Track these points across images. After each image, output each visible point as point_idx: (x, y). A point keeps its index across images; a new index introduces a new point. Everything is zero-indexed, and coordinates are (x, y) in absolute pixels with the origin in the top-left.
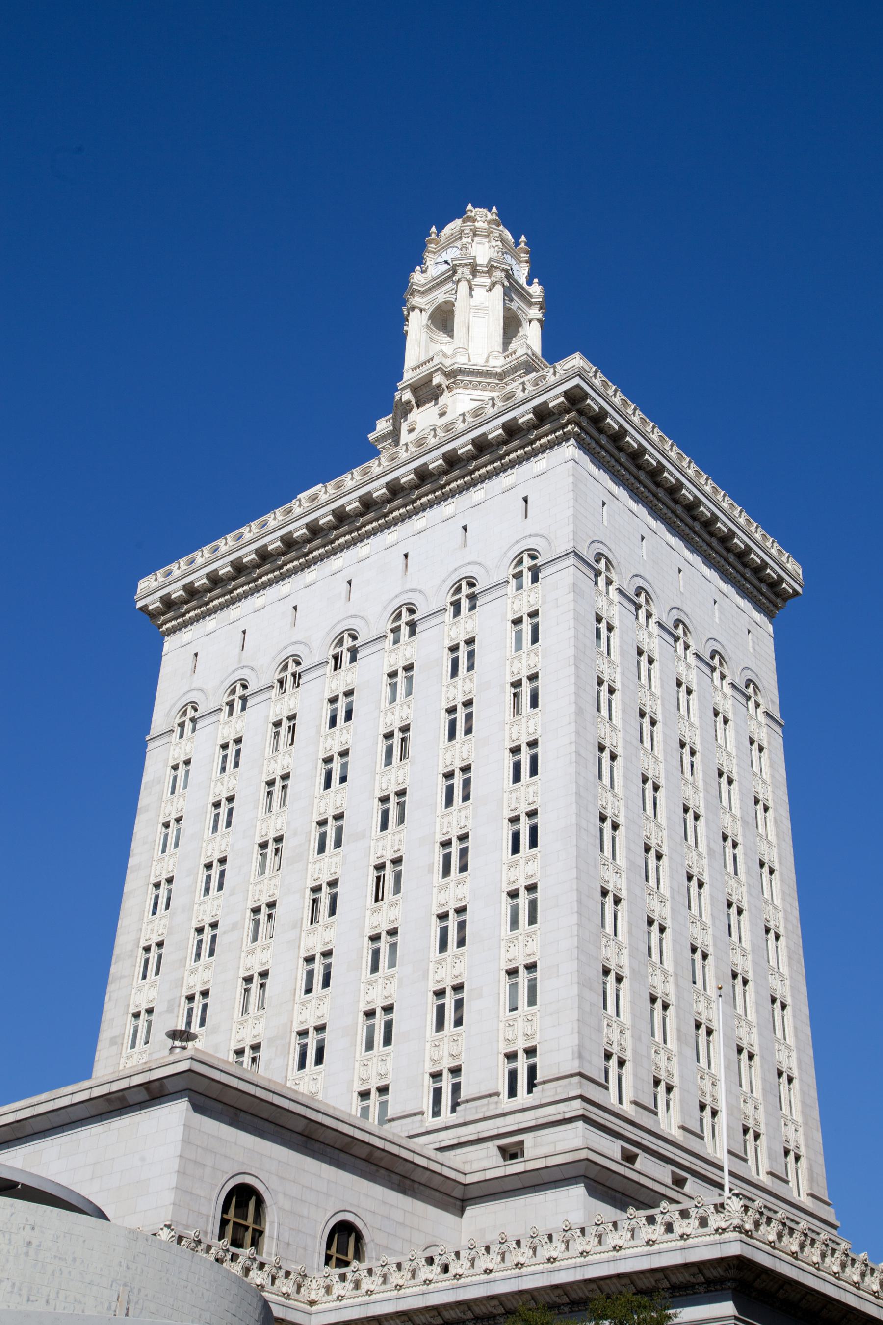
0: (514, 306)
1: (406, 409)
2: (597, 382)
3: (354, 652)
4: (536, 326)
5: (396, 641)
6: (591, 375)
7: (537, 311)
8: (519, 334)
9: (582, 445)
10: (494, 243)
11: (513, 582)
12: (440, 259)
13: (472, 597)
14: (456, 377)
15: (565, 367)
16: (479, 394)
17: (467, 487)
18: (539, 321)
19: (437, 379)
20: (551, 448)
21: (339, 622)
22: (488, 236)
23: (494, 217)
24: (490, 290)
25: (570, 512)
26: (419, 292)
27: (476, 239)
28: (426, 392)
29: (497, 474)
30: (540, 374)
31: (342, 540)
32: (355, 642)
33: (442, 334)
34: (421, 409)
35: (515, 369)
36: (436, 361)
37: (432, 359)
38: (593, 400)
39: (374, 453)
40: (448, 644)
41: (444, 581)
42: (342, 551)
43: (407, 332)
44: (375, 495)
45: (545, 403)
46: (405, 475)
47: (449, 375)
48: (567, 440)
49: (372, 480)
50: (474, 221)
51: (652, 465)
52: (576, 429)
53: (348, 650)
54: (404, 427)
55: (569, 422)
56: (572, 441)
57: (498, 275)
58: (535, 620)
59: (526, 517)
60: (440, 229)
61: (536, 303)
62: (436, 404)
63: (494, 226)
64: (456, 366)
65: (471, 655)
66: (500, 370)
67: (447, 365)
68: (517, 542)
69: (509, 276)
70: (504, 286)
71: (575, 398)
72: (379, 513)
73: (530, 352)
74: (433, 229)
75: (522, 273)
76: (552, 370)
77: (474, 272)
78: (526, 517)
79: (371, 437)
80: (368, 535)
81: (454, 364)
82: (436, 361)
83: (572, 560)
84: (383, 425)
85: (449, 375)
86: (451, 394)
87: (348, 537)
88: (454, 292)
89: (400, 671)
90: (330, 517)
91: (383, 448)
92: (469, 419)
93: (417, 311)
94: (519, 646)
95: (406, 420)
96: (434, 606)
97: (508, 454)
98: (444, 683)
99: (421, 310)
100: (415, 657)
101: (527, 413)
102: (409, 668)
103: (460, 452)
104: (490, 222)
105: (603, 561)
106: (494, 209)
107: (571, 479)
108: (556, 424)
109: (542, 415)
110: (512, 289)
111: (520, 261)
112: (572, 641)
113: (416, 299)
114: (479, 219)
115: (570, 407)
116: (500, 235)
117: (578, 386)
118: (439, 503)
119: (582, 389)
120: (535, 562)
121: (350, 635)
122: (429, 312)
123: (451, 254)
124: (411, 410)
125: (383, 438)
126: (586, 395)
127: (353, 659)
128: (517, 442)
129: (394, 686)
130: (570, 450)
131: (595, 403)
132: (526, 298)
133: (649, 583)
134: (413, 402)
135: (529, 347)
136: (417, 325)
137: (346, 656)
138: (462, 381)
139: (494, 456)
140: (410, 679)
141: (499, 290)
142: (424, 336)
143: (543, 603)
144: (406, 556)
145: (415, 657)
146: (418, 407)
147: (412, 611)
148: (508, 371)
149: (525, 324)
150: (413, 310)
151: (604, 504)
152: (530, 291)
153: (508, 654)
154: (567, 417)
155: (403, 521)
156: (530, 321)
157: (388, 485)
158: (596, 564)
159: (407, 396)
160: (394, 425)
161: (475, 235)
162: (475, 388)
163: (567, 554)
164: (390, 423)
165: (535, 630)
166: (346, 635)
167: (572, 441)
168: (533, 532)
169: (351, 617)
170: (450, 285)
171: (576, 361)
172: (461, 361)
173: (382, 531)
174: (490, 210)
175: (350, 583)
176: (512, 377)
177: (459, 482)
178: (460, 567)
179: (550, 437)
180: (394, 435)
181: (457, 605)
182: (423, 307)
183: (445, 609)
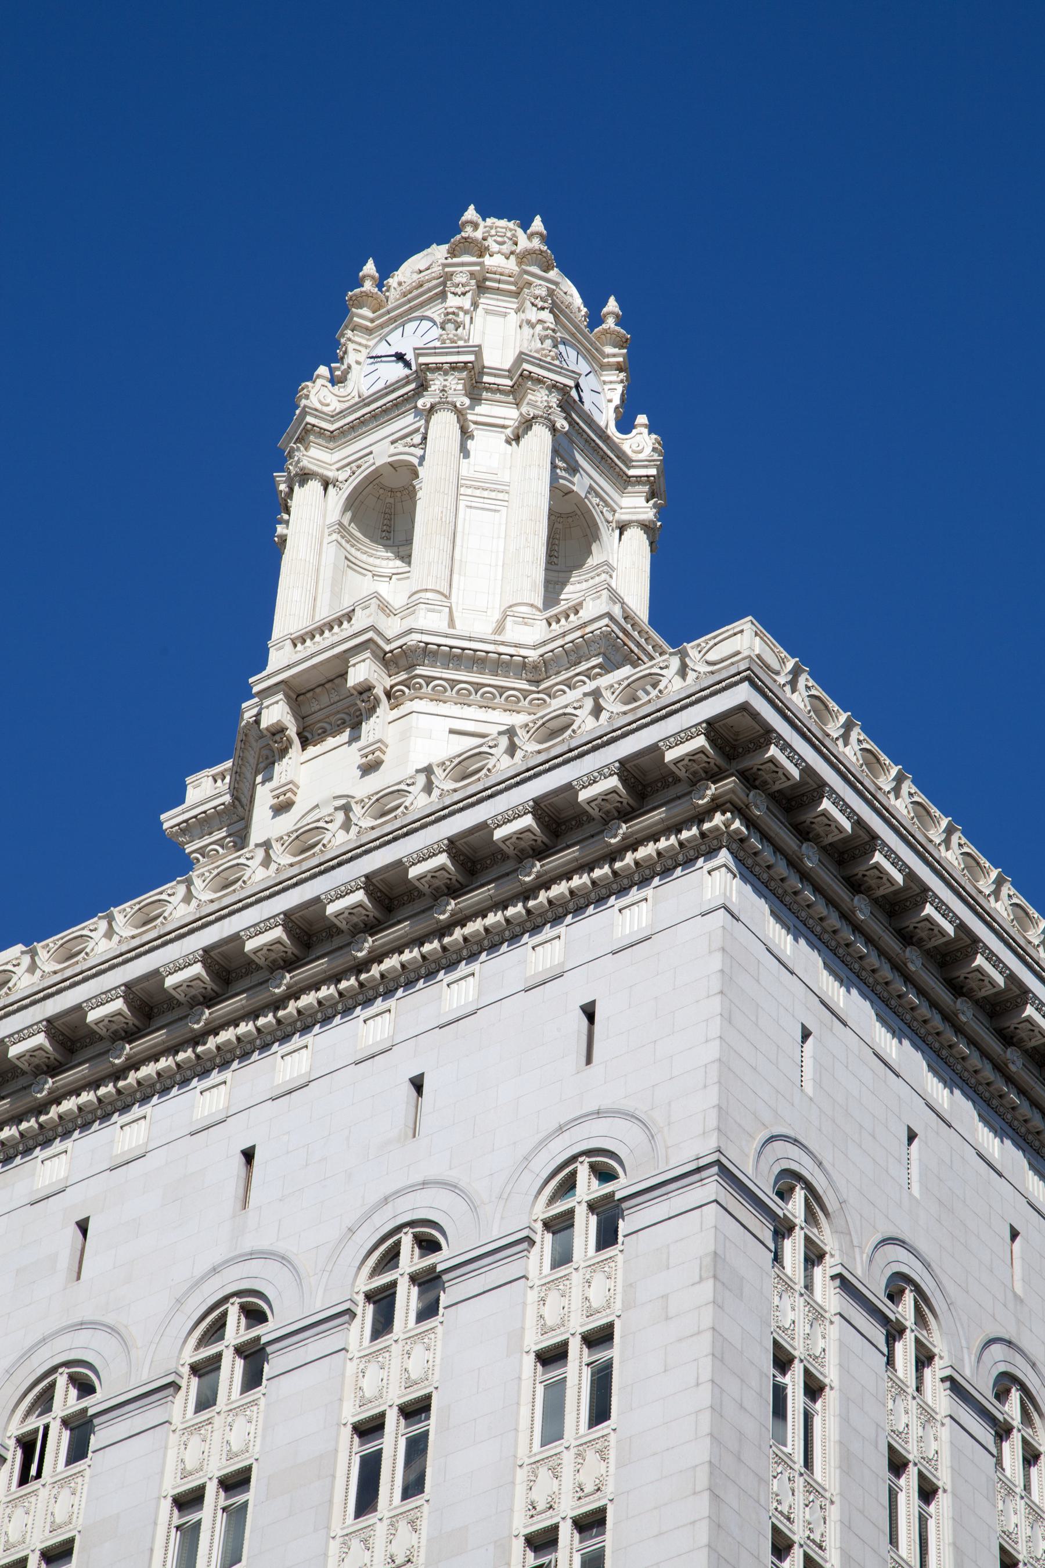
0: (579, 485)
1: (271, 748)
2: (798, 701)
3: (81, 1429)
4: (637, 544)
5: (206, 1402)
6: (782, 679)
7: (641, 501)
8: (591, 562)
9: (749, 869)
10: (533, 315)
11: (546, 1242)
12: (383, 349)
13: (429, 1282)
14: (412, 667)
15: (712, 656)
17: (428, 970)
18: (647, 527)
19: (362, 671)
20: (666, 872)
21: (44, 1340)
22: (517, 294)
23: (536, 243)
24: (517, 439)
25: (713, 1050)
26: (321, 433)
28: (330, 706)
29: (514, 938)
30: (642, 670)
31: (69, 1105)
32: (87, 1402)
33: (382, 552)
34: (312, 751)
35: (573, 655)
36: (360, 621)
37: (349, 616)
38: (785, 746)
39: (175, 864)
40: (352, 1413)
41: (352, 1231)
42: (66, 1134)
43: (284, 539)
44: (170, 981)
45: (654, 751)
46: (258, 928)
48: (711, 853)
49: (165, 940)
50: (482, 251)
51: (942, 933)
52: (737, 824)
53: (65, 1422)
54: (264, 797)
55: (717, 805)
56: (724, 856)
57: (540, 398)
58: (602, 1355)
59: (589, 1061)
60: (386, 269)
61: (639, 480)
62: (355, 738)
64: (413, 639)
65: (417, 1448)
66: (533, 655)
67: (390, 634)
68: (561, 1129)
69: (570, 404)
70: (553, 429)
71: (736, 741)
72: (180, 1032)
73: (617, 611)
74: (370, 268)
76: (675, 663)
77: (476, 390)
78: (589, 1061)
79: (170, 819)
80: (145, 1093)
81: (410, 631)
82: (360, 621)
83: (711, 1187)
84: (205, 790)
87: (87, 1097)
88: (417, 439)
89: (212, 1491)
90: (40, 1039)
91: (202, 851)
92: (444, 783)
93: (314, 486)
94: (553, 1427)
95: (268, 779)
96: (321, 1301)
98: (337, 1530)
99: (326, 484)
100: (256, 1450)
101: (602, 773)
102: (236, 1482)
103: (414, 872)
104: (523, 258)
105: (799, 1195)
107: (716, 962)
108: (680, 809)
109: (645, 782)
110: (577, 440)
111: (603, 367)
112: (706, 1418)
113: (315, 452)
114: (495, 248)
115: (720, 761)
116: (551, 293)
117: (745, 708)
118: (347, 1011)
119: (755, 716)
120: (608, 1188)
121: (73, 1379)
122: (348, 489)
124: (284, 752)
125: (204, 824)
126: (767, 735)
127: (78, 1452)
128: (571, 853)
129: (190, 1535)
130: (716, 881)
131: (790, 756)
132: (614, 466)
133: (927, 1266)
134: (292, 732)
135: (615, 597)
136: (311, 522)
137: (59, 1442)
138: (429, 680)
139: (508, 888)
140: (236, 1516)
141: (540, 439)
142: (331, 553)
143: (627, 1306)
144: (249, 1155)
145: (256, 1450)
146: (305, 743)
147: (255, 1316)
148: (556, 659)
149: (609, 536)
150: (302, 483)
151: (806, 1034)
152: (626, 447)
153: (522, 1451)
154: (712, 790)
155: (245, 1055)
156: (622, 528)
157: (208, 956)
158: (781, 1204)
159: (277, 713)
160: (235, 791)
161: (482, 288)
163: (699, 1170)
164: (223, 785)
165: (602, 1382)
166: (62, 1380)
167: (724, 856)
168: (606, 1103)
169: (81, 1326)
170: (407, 421)
171: (744, 640)
173: (185, 1082)
174: (525, 226)
175: (83, 1227)
177: (407, 956)
178: (399, 1193)
179: (663, 844)
180: (235, 818)
181: (383, 1301)
182: (330, 474)
183: (350, 1313)
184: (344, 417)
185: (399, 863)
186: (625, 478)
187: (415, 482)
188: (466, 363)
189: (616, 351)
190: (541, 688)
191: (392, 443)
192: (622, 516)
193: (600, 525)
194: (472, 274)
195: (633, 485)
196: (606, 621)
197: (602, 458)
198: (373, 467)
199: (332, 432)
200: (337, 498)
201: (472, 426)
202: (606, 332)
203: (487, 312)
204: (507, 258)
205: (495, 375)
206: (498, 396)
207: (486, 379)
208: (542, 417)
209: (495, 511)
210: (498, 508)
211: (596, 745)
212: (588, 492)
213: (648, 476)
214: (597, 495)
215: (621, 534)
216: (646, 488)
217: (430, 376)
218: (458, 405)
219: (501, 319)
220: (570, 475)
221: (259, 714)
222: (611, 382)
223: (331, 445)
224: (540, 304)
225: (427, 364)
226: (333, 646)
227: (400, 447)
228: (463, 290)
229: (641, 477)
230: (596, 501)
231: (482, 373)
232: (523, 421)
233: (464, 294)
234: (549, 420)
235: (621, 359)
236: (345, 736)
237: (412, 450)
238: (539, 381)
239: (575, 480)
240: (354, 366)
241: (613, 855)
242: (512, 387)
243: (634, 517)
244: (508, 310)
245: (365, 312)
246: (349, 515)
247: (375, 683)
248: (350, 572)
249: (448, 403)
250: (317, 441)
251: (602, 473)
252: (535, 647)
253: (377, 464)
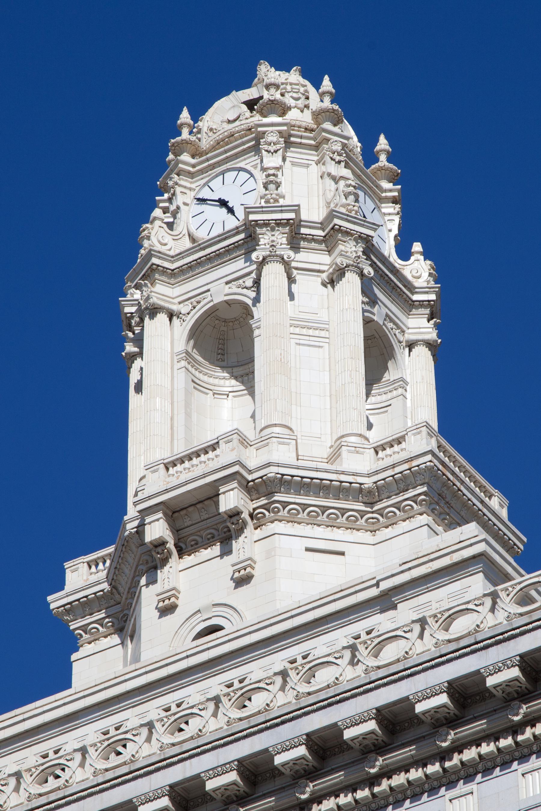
0: (378, 314)
12: (205, 194)
14: (270, 494)
18: (429, 345)
19: (231, 499)
22: (316, 148)
23: (327, 103)
26: (164, 271)
27: (293, 154)
28: (201, 522)
33: (220, 373)
34: (188, 560)
35: (402, 483)
36: (225, 455)
37: (214, 447)
46: (217, 771)
47: (255, 488)
54: (149, 597)
60: (197, 114)
61: (421, 304)
62: (226, 552)
63: (328, 126)
66: (368, 482)
69: (370, 249)
70: (362, 275)
74: (185, 116)
75: (388, 226)
77: (296, 241)
79: (56, 601)
81: (269, 465)
84: (83, 577)
85: (255, 488)
86: (259, 533)
88: (249, 282)
91: (84, 628)
93: (162, 317)
97: (459, 747)
99: (171, 315)
101: (505, 664)
104: (318, 115)
106: (327, 84)
111: (382, 200)
116: (344, 146)
123: (241, 189)
124: (165, 561)
125: (85, 606)
128: (480, 725)
132: (398, 289)
134: (171, 545)
136: (162, 351)
138: (285, 504)
141: (351, 283)
142: (181, 377)
146: (181, 553)
148: (387, 486)
149: (402, 353)
150: (152, 317)
152: (407, 273)
156: (411, 346)
159: (157, 529)
160: (113, 579)
161: (288, 144)
164: (101, 573)
170: (238, 265)
172: (279, 457)
174: (317, 85)
176: (395, 500)
182: (175, 308)
184: (183, 258)
186: (410, 302)
187: (251, 322)
188: (288, 220)
189: (390, 186)
190: (376, 508)
191: (227, 283)
192: (410, 336)
193: (395, 346)
195: (417, 308)
196: (429, 457)
197: (393, 288)
198: (211, 304)
199: (173, 270)
200: (182, 329)
201: (295, 272)
202: (381, 169)
203: (293, 164)
204: (302, 111)
205: (310, 227)
206: (313, 245)
207: (303, 231)
208: (352, 266)
209: (319, 347)
210: (321, 344)
212: (385, 320)
213: (429, 301)
214: (392, 321)
215: (410, 351)
216: (428, 311)
217: (259, 230)
218: (285, 258)
219: (304, 170)
220: (371, 307)
221: (142, 525)
222: (389, 214)
223: (172, 281)
224: (338, 158)
225: (256, 221)
226: (204, 476)
227: (234, 288)
229: (423, 301)
230: (390, 325)
231: (300, 226)
232: (337, 269)
233: (276, 152)
234: (359, 268)
235: (396, 194)
236: (216, 549)
237: (245, 291)
238: (348, 233)
239: (375, 310)
240: (182, 207)
241: (515, 730)
242: (325, 237)
244: (310, 162)
245: (185, 157)
246: (192, 342)
247: (242, 509)
248: (196, 392)
249: (277, 256)
250: (160, 278)
251: (393, 301)
252: (369, 475)
253: (216, 301)
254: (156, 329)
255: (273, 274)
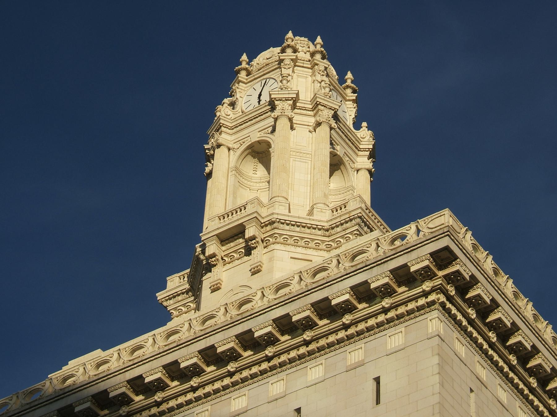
6: (461, 236)
10: (319, 78)
15: (431, 225)
16: (300, 252)
25: (436, 399)
36: (250, 209)
39: (162, 316)
43: (210, 175)
49: (180, 346)
50: (295, 51)
59: (378, 402)
60: (251, 58)
67: (263, 215)
69: (336, 117)
73: (363, 206)
74: (244, 57)
75: (349, 112)
78: (378, 402)
79: (160, 296)
81: (273, 214)
82: (250, 209)
84: (176, 282)
91: (175, 309)
93: (223, 149)
99: (229, 149)
106: (319, 40)
114: (300, 49)
122: (239, 152)
135: (363, 201)
138: (281, 235)
141: (324, 130)
162: (296, 244)
171: (445, 218)
182: (231, 146)
185: (288, 315)
187: (270, 149)
188: (292, 98)
191: (259, 132)
194: (292, 60)
196: (360, 211)
198: (250, 143)
204: (305, 53)
209: (306, 162)
211: (379, 263)
216: (368, 153)
217: (276, 103)
224: (322, 73)
226: (238, 220)
228: (289, 67)
235: (355, 98)
237: (268, 135)
240: (240, 99)
243: (363, 167)
247: (257, 236)
248: (240, 188)
252: (327, 222)
254: (221, 155)
255: (283, 124)
